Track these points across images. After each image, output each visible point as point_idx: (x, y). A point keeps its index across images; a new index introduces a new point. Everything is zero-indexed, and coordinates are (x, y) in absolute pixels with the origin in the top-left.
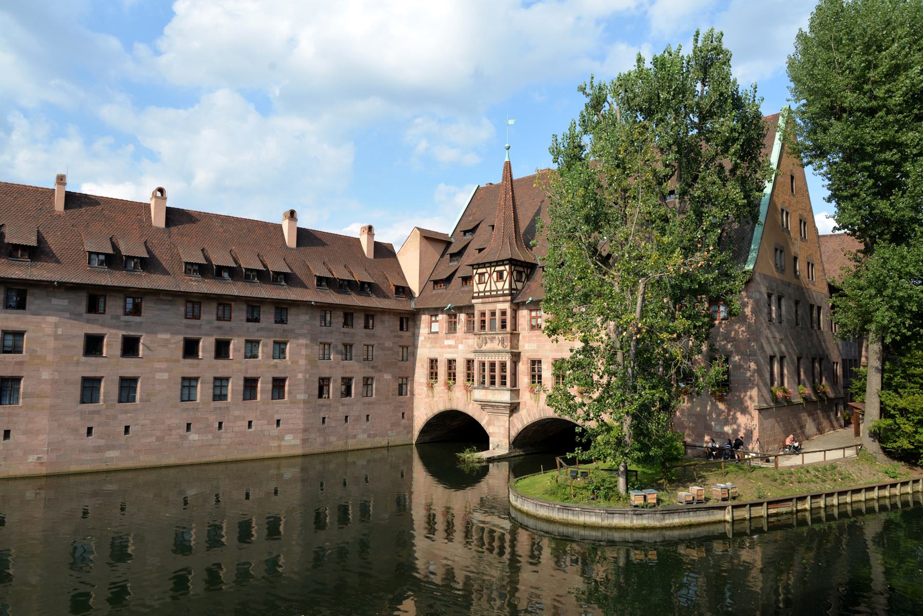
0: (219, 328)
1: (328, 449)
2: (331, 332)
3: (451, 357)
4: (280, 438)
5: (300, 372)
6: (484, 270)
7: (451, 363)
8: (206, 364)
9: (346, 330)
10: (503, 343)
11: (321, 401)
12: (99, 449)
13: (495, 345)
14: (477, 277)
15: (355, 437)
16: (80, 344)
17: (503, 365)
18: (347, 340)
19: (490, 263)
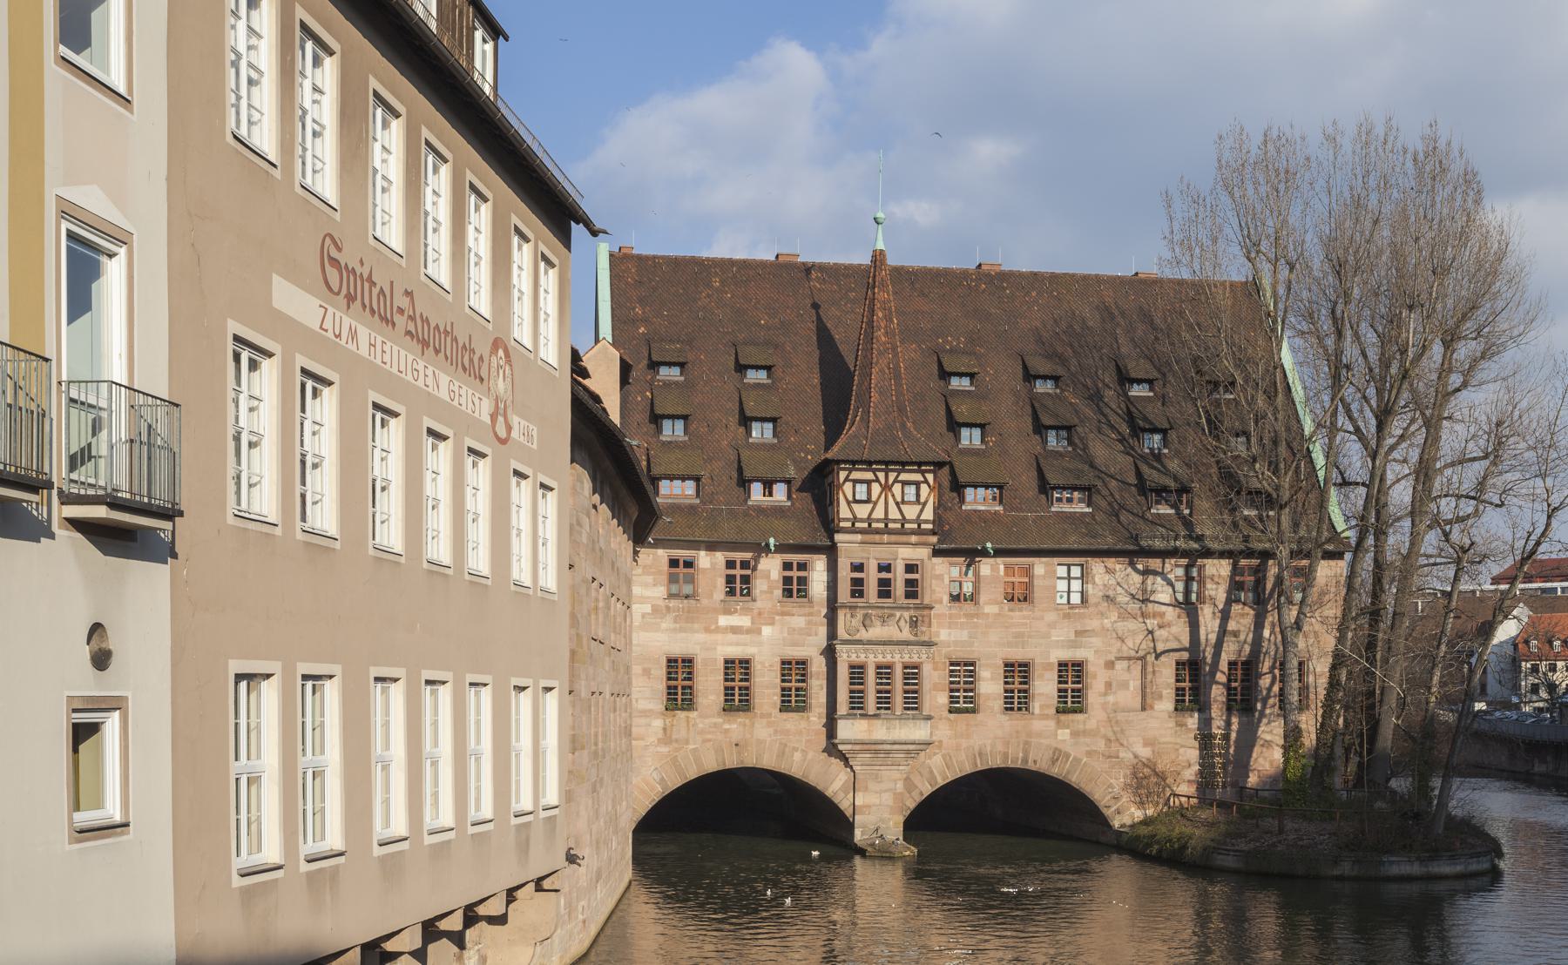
3: (735, 652)
6: (869, 476)
14: (848, 485)
17: (912, 673)
19: (887, 463)
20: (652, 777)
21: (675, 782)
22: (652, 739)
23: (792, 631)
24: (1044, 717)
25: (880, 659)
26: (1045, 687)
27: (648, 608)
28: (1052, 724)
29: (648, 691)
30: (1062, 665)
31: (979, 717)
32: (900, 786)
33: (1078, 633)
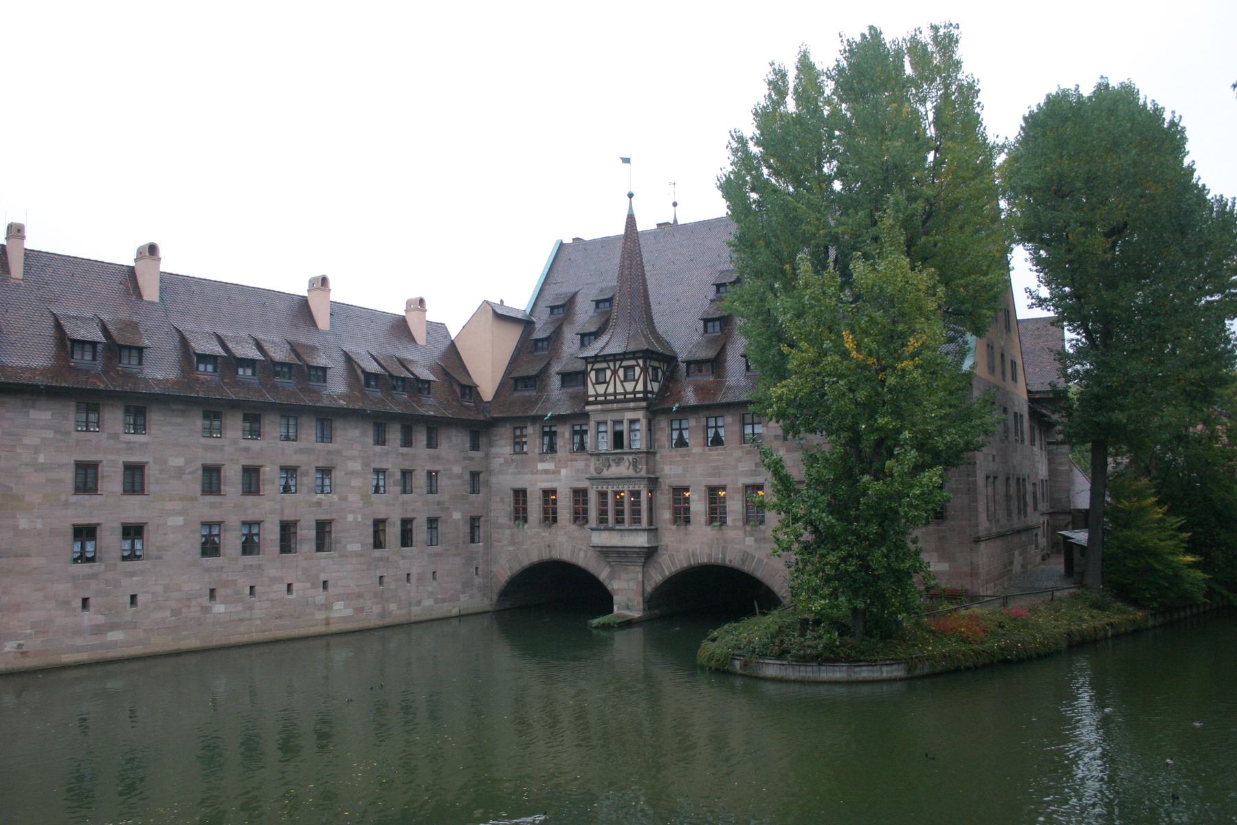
0: (247, 449)
1: (388, 621)
2: (387, 454)
4: (327, 607)
5: (352, 512)
6: (604, 365)
8: (232, 506)
9: (405, 450)
10: (635, 466)
11: (378, 553)
12: (97, 630)
13: (623, 469)
14: (593, 374)
15: (419, 603)
16: (68, 476)
17: (636, 494)
18: (407, 465)
19: (614, 355)
21: (517, 568)
22: (505, 542)
23: (578, 471)
24: (738, 528)
25: (615, 489)
27: (502, 460)
28: (741, 533)
29: (502, 510)
30: (747, 487)
32: (640, 576)
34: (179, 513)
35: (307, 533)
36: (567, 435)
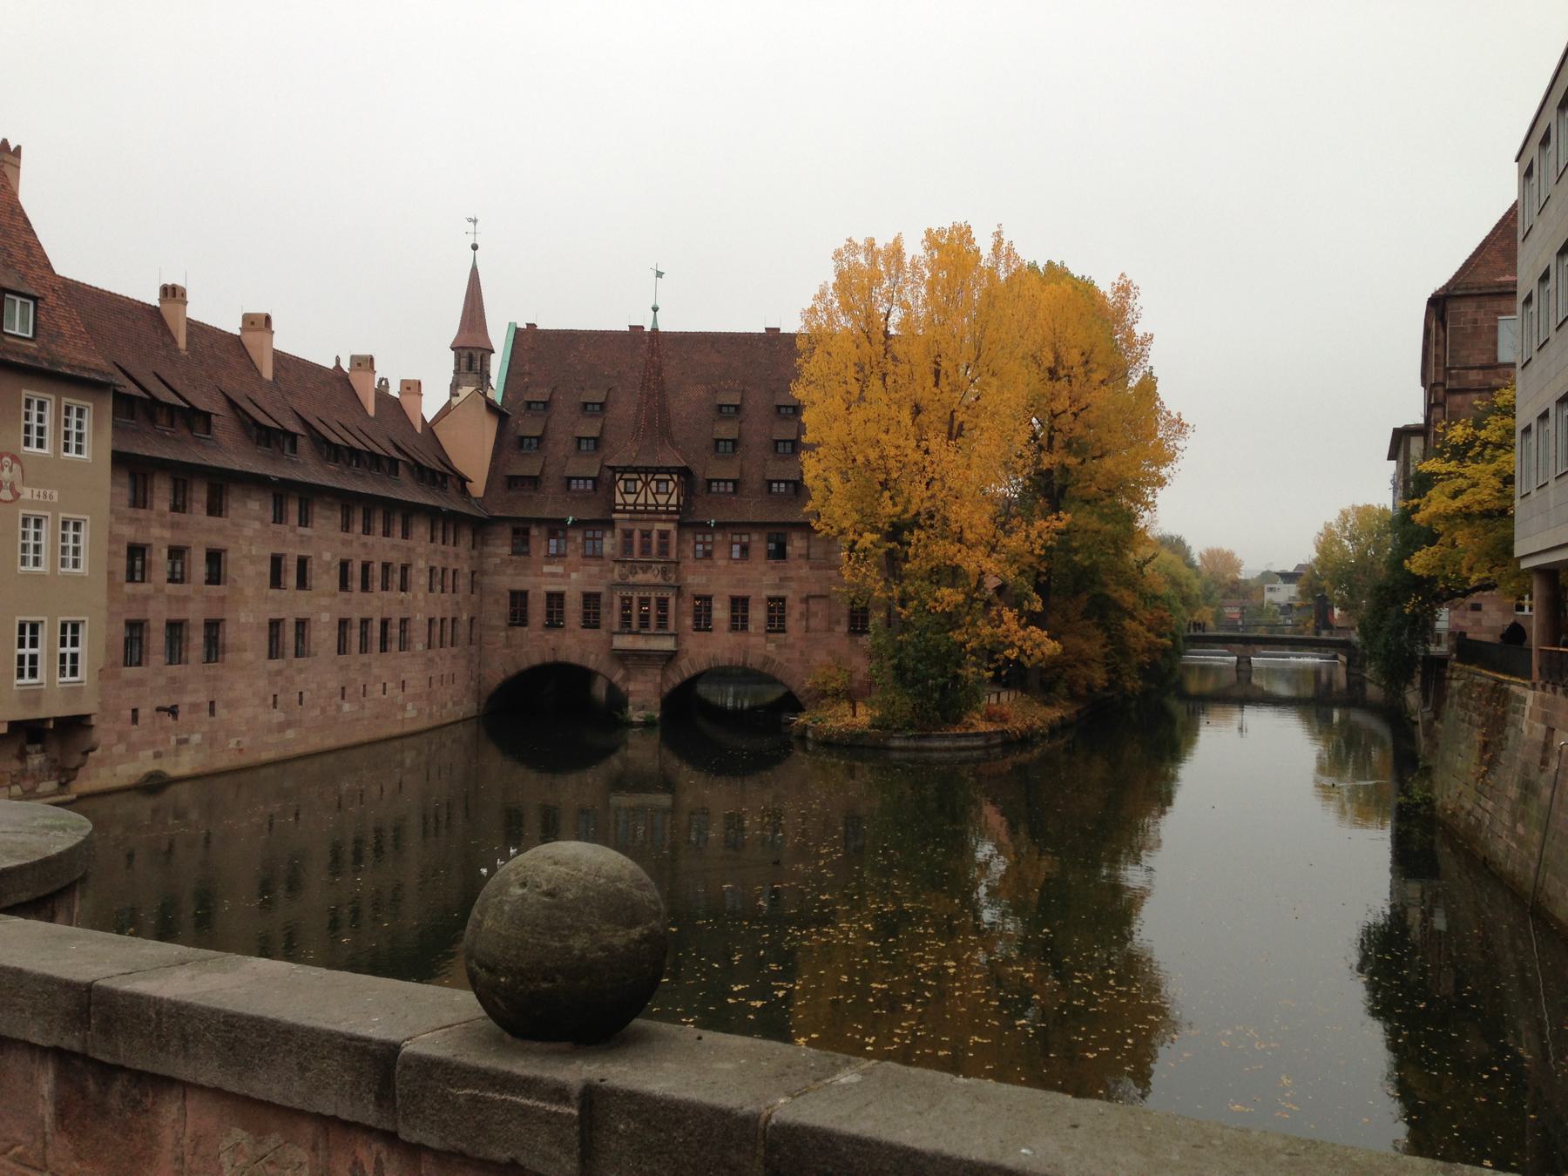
4: (403, 708)
6: (635, 476)
7: (555, 600)
9: (443, 548)
11: (431, 653)
12: (282, 727)
13: (652, 577)
16: (266, 568)
17: (663, 604)
20: (499, 669)
21: (512, 671)
24: (757, 635)
26: (758, 615)
27: (498, 561)
29: (498, 612)
30: (770, 599)
31: (714, 634)
32: (659, 679)
33: (781, 579)
34: (327, 609)
35: (394, 632)
36: (579, 540)
